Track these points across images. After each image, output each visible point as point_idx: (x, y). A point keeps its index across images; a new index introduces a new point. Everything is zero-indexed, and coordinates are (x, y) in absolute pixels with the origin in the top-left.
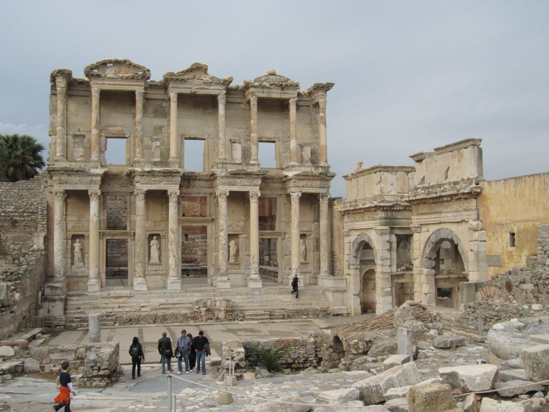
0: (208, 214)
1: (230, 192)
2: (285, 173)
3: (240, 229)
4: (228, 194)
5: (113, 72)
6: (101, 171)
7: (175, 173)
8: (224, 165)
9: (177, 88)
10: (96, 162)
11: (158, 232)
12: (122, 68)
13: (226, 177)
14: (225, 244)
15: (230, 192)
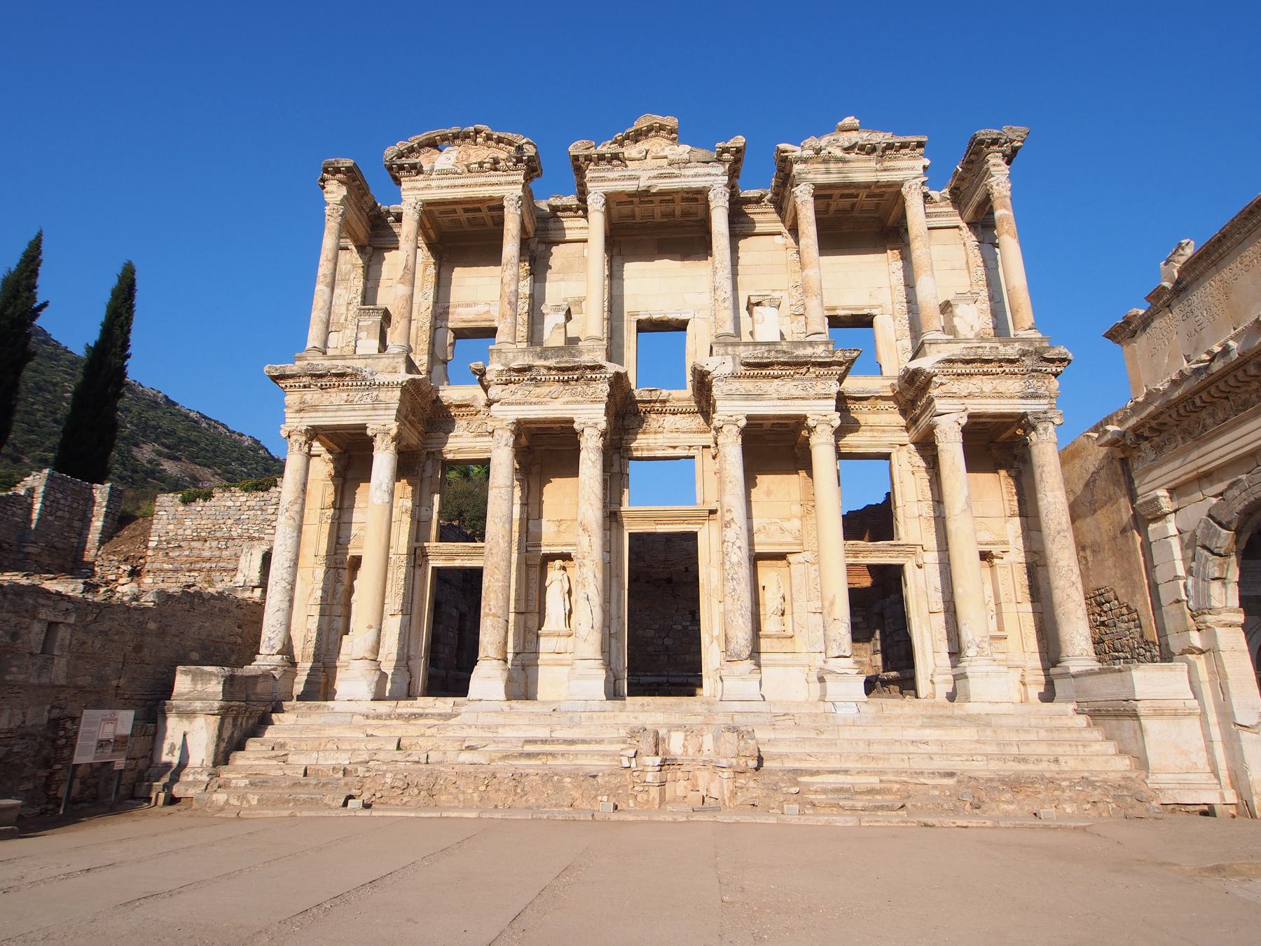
0: (699, 499)
1: (749, 418)
2: (914, 365)
3: (790, 540)
4: (743, 423)
5: (453, 160)
6: (403, 376)
7: (593, 368)
8: (730, 349)
9: (603, 179)
10: (395, 356)
11: (565, 550)
12: (471, 152)
13: (735, 376)
14: (739, 563)
15: (749, 418)
